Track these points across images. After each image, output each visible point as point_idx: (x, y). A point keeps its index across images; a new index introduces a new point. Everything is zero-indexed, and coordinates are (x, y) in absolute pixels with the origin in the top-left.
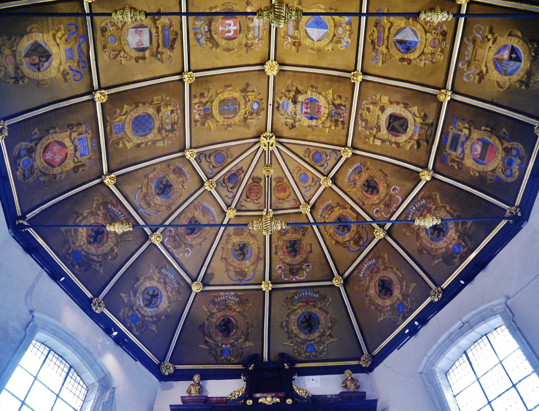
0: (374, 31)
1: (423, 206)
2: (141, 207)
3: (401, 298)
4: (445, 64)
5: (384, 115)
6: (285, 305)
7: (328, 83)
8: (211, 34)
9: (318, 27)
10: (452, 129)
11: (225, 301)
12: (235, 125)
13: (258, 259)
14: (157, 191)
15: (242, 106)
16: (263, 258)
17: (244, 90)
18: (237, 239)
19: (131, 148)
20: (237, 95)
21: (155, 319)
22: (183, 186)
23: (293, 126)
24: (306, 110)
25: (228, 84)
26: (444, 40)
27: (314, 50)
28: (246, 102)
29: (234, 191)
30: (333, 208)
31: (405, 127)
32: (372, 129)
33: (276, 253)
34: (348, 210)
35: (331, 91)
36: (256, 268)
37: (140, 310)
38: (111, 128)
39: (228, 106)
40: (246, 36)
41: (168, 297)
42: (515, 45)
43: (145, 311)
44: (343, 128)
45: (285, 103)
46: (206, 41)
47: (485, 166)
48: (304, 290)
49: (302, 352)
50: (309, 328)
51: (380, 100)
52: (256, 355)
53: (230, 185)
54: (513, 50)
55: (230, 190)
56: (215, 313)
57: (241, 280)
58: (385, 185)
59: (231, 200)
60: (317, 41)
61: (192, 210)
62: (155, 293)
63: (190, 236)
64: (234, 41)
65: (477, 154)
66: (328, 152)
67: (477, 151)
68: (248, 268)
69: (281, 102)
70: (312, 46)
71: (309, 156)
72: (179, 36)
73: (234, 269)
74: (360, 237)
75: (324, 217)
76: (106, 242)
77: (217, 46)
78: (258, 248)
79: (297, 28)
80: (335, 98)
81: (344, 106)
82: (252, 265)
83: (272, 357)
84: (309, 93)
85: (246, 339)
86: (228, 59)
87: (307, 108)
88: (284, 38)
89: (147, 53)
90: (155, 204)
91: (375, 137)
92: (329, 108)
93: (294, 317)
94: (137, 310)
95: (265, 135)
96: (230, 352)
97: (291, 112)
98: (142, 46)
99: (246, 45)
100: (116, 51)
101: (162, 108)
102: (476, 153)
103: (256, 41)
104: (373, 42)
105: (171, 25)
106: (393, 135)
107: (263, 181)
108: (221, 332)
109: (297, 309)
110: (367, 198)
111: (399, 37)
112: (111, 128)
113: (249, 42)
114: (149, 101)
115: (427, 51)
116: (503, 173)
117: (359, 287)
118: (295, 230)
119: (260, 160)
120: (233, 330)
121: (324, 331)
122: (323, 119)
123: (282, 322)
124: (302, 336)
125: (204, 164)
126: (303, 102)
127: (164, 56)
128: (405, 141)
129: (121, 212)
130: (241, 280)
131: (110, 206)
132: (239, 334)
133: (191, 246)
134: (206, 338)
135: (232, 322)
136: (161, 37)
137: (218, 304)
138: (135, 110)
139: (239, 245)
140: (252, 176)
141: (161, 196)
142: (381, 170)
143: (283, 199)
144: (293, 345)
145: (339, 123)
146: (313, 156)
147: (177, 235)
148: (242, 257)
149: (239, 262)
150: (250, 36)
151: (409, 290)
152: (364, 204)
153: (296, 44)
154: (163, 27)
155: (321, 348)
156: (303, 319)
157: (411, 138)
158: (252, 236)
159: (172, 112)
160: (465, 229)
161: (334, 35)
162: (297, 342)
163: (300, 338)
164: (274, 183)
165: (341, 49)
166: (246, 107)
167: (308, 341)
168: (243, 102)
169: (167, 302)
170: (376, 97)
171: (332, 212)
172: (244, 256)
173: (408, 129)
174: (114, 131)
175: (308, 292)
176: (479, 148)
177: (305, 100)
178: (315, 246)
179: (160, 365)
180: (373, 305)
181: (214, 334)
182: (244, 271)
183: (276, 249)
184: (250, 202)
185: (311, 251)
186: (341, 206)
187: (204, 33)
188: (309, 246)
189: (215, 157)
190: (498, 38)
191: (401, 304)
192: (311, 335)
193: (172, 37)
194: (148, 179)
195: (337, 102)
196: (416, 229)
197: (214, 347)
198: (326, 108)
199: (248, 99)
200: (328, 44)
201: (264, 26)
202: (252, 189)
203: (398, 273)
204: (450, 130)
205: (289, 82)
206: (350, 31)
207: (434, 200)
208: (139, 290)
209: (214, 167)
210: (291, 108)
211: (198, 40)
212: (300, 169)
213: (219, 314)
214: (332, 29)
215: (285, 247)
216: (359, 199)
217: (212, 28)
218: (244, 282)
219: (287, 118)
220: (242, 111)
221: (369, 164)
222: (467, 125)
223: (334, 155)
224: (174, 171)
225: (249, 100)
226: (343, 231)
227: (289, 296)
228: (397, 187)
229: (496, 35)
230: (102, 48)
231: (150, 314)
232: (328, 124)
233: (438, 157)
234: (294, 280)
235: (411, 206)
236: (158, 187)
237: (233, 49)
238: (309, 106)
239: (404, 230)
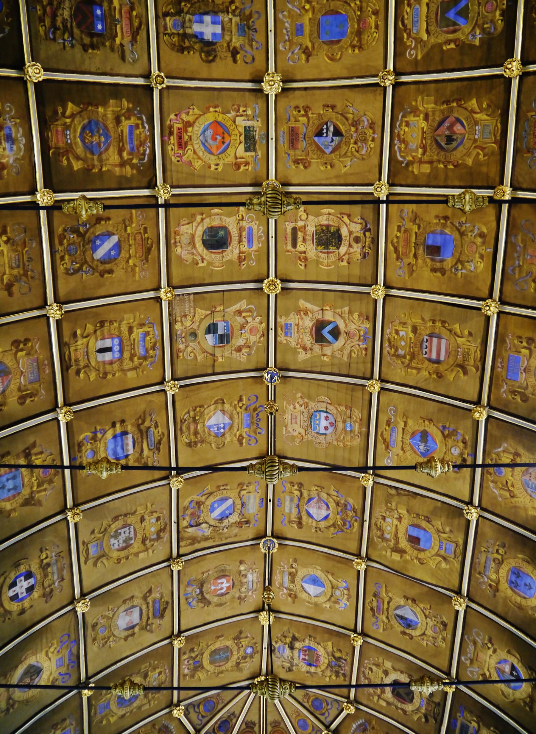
4: (448, 652)
7: (326, 636)
9: (314, 584)
12: (227, 670)
15: (235, 653)
17: (237, 638)
19: (115, 722)
23: (290, 670)
24: (304, 657)
25: (220, 634)
28: (239, 648)
31: (411, 697)
35: (330, 644)
39: (220, 655)
42: (515, 664)
45: (281, 647)
46: (197, 602)
54: (513, 668)
64: (227, 596)
66: (329, 701)
69: (277, 646)
71: (308, 701)
72: (170, 605)
77: (209, 603)
79: (293, 581)
81: (345, 660)
84: (307, 641)
87: (305, 655)
88: (279, 588)
89: (136, 629)
91: (379, 697)
100: (105, 638)
101: (149, 673)
103: (250, 593)
104: (372, 609)
105: (162, 597)
106: (399, 701)
107: (257, 725)
113: (243, 595)
114: (136, 672)
119: (254, 703)
122: (323, 668)
125: (193, 716)
126: (300, 650)
127: (154, 626)
128: (412, 711)
140: (245, 720)
145: (340, 675)
146: (312, 702)
150: (243, 590)
153: (292, 596)
154: (154, 601)
157: (418, 709)
159: (160, 673)
161: (332, 596)
164: (269, 729)
166: (238, 652)
173: (414, 700)
174: (98, 711)
189: (205, 706)
190: (498, 650)
195: (338, 655)
201: (258, 579)
205: (285, 628)
206: (348, 595)
209: (203, 717)
211: (189, 604)
212: (299, 715)
217: (204, 589)
219: (283, 661)
220: (234, 658)
221: (374, 723)
223: (335, 705)
225: (242, 646)
229: (495, 646)
232: (328, 673)
237: (226, 603)
238: (307, 653)
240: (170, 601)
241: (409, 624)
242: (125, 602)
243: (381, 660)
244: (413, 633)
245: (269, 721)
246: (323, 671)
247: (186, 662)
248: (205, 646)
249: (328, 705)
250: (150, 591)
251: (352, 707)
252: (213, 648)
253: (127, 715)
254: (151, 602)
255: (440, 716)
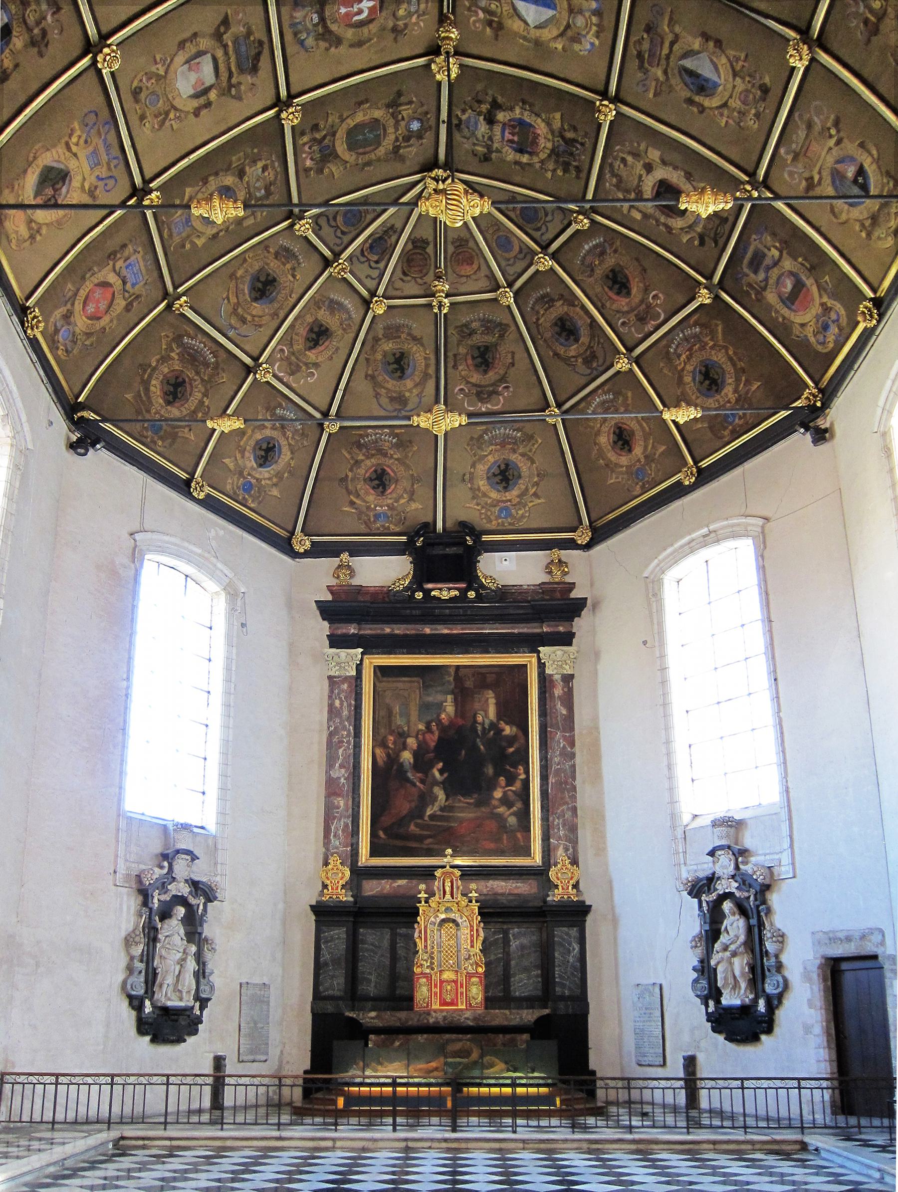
0: (643, 38)
1: (695, 336)
2: (232, 327)
3: (643, 460)
5: (650, 177)
6: (469, 449)
8: (325, 27)
10: (755, 240)
11: (377, 442)
13: (426, 376)
14: (254, 294)
15: (391, 130)
16: (434, 376)
17: (393, 105)
18: (390, 345)
20: (378, 114)
21: (275, 480)
22: (294, 276)
23: (486, 158)
24: (511, 137)
25: (363, 98)
26: (764, 100)
27: (529, 42)
28: (397, 122)
29: (382, 265)
30: (553, 300)
32: (628, 191)
33: (455, 367)
34: (578, 309)
35: (558, 116)
36: (422, 391)
37: (253, 473)
38: (170, 229)
40: (394, 15)
41: (290, 445)
43: (261, 473)
44: (578, 177)
46: (316, 40)
47: (793, 314)
48: (498, 426)
49: (492, 518)
50: (504, 484)
51: (646, 152)
52: (425, 525)
53: (376, 258)
55: (373, 264)
56: (363, 461)
57: (400, 410)
58: (641, 285)
59: (377, 281)
60: (535, 27)
61: (312, 310)
62: (271, 445)
63: (313, 351)
64: (371, 26)
65: (786, 293)
67: (785, 287)
68: (410, 391)
69: (464, 117)
70: (525, 34)
73: (387, 393)
74: (594, 356)
75: (538, 312)
76: (190, 395)
77: (338, 41)
78: (425, 358)
80: (566, 127)
81: (582, 144)
82: (416, 386)
83: (448, 525)
84: (518, 110)
85: (411, 499)
86: (362, 57)
87: (513, 134)
88: (469, 9)
89: (213, 95)
90: (254, 316)
92: (553, 141)
93: (481, 469)
94: (249, 474)
95: (433, 174)
96: (388, 517)
97: (483, 136)
98: (203, 87)
99: (394, 30)
100: (160, 114)
101: (247, 168)
102: (783, 289)
104: (640, 56)
107: (431, 246)
108: (374, 488)
109: (487, 456)
110: (610, 298)
111: (688, 63)
112: (170, 229)
113: (400, 23)
115: (731, 103)
116: (815, 336)
117: (586, 428)
118: (487, 328)
120: (390, 486)
121: (527, 489)
122: (543, 156)
123: (464, 475)
124: (494, 495)
125: (326, 230)
126: (504, 124)
127: (243, 88)
128: (682, 229)
129: (204, 343)
130: (400, 410)
131: (186, 340)
132: (400, 492)
133: (316, 365)
134: (352, 497)
135: (388, 474)
136: (233, 59)
137: (366, 448)
138: (203, 190)
139: (394, 355)
140: (412, 237)
141: (260, 302)
142: (637, 259)
143: (467, 276)
144: (479, 508)
147: (293, 354)
148: (399, 374)
149: (395, 382)
150: (401, 12)
151: (655, 454)
152: (603, 305)
153: (495, 25)
154: (236, 42)
155: (520, 512)
156: (495, 470)
157: (690, 227)
158: (414, 339)
159: (265, 168)
160: (747, 393)
161: (568, 26)
162: (486, 504)
163: (490, 498)
165: (582, 53)
166: (397, 129)
167: (503, 501)
168: (392, 122)
169: (289, 453)
170: (639, 145)
171: (550, 307)
172: (403, 372)
174: (175, 231)
175: (505, 429)
176: (789, 285)
177: (510, 120)
178: (520, 355)
179: (290, 539)
180: (603, 459)
181: (363, 491)
182: (404, 396)
183: (455, 362)
184: (409, 281)
185: (513, 364)
186: (565, 300)
187: (310, 27)
188: (510, 356)
191: (641, 470)
192: (507, 494)
193: (253, 52)
194: (237, 279)
195: (570, 135)
196: (679, 368)
197: (364, 509)
198: (549, 140)
199: (400, 117)
200: (558, 36)
202: (412, 260)
203: (645, 425)
204: (752, 240)
205: (479, 87)
207: (713, 334)
208: (248, 448)
209: (343, 233)
210: (483, 129)
211: (302, 43)
212: (498, 230)
213: (368, 463)
214: (565, 14)
215: (469, 357)
216: (596, 296)
217: (327, 13)
218: (404, 413)
219: (474, 144)
221: (618, 243)
222: (778, 245)
224: (277, 255)
225: (403, 119)
226: (566, 340)
227: (476, 436)
228: (660, 295)
230: (138, 122)
231: (267, 475)
233: (730, 271)
234: (483, 409)
235: (676, 331)
236: (254, 289)
237: (370, 40)
239: (662, 365)
240: (265, 39)
241: (702, 86)
242: (182, 45)
243: (643, 146)
244: (707, 103)
245: (450, 239)
246: (542, 162)
247: (306, 148)
248: (337, 121)
249: (546, 215)
250: (225, 22)
251: (585, 221)
252: (351, 123)
253: (221, 234)
254: (230, 44)
255: (725, 237)
